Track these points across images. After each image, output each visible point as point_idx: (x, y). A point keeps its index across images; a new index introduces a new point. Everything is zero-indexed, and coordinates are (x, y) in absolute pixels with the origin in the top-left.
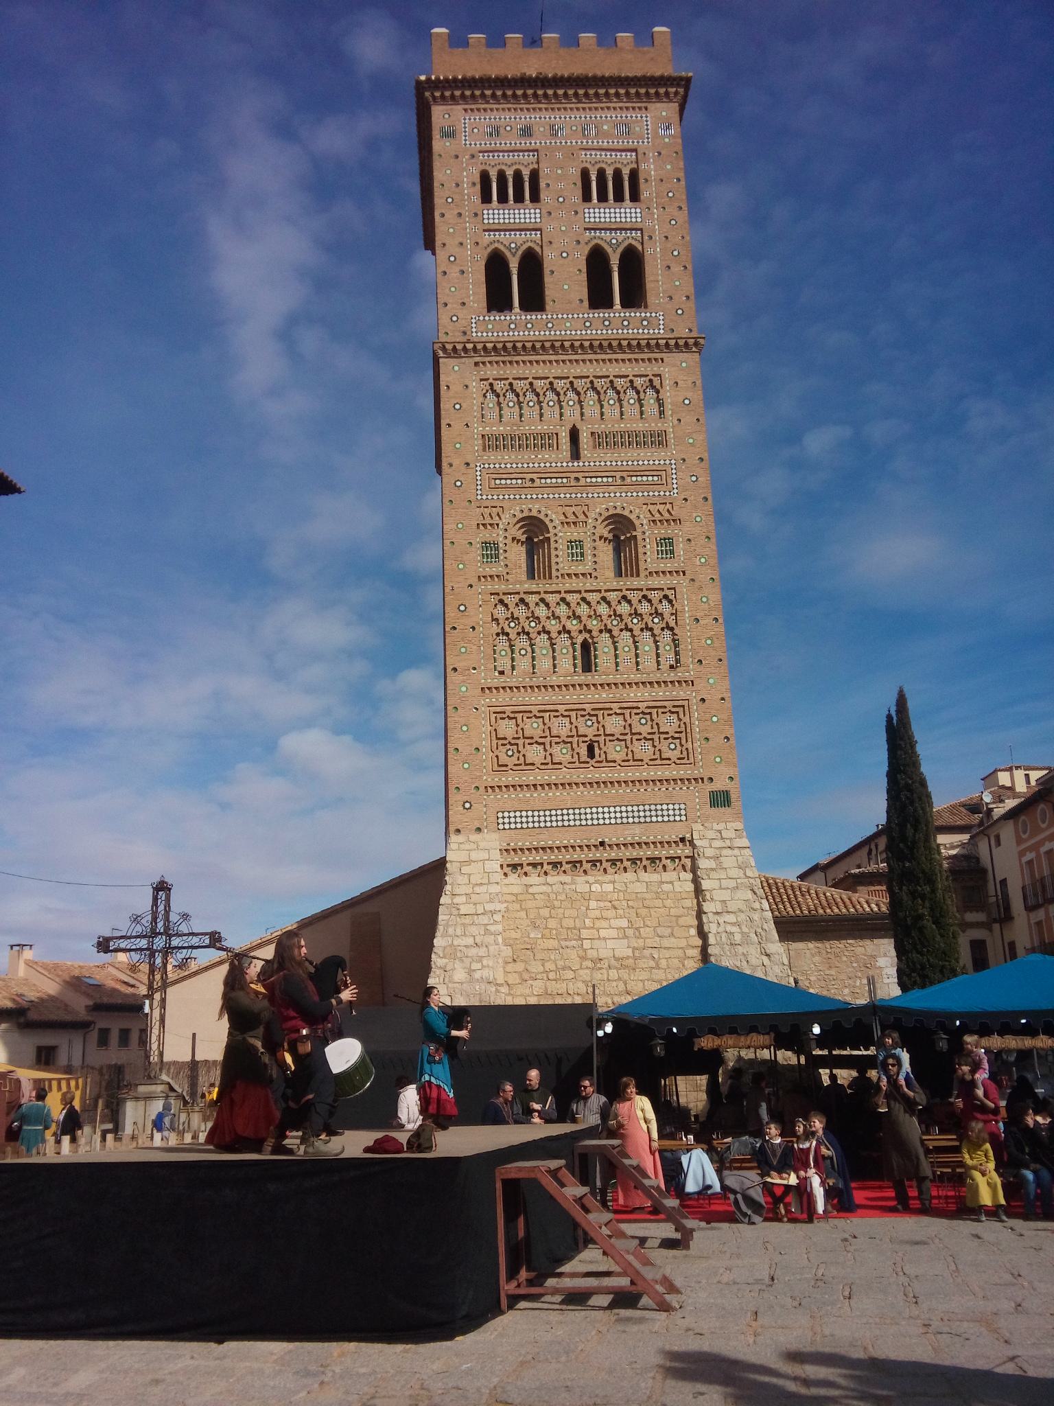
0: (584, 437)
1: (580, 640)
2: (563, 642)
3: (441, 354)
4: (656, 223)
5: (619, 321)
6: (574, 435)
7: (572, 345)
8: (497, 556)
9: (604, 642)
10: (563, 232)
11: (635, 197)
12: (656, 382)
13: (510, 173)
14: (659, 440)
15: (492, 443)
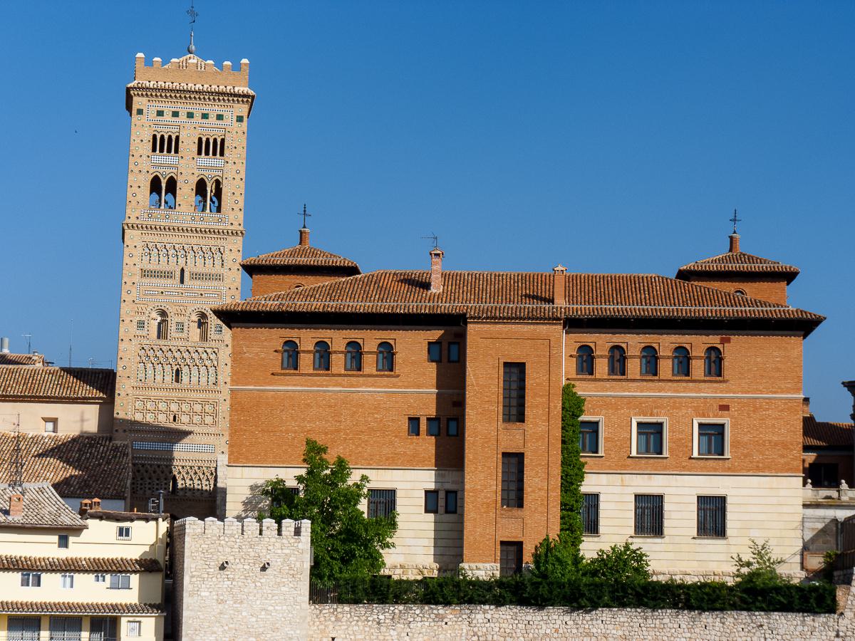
0: (187, 275)
1: (175, 368)
2: (168, 368)
3: (126, 227)
4: (232, 171)
5: (209, 219)
6: (182, 271)
7: (187, 229)
8: (143, 327)
9: (185, 370)
10: (188, 167)
11: (222, 154)
12: (222, 250)
13: (166, 137)
14: (219, 278)
15: (145, 273)
